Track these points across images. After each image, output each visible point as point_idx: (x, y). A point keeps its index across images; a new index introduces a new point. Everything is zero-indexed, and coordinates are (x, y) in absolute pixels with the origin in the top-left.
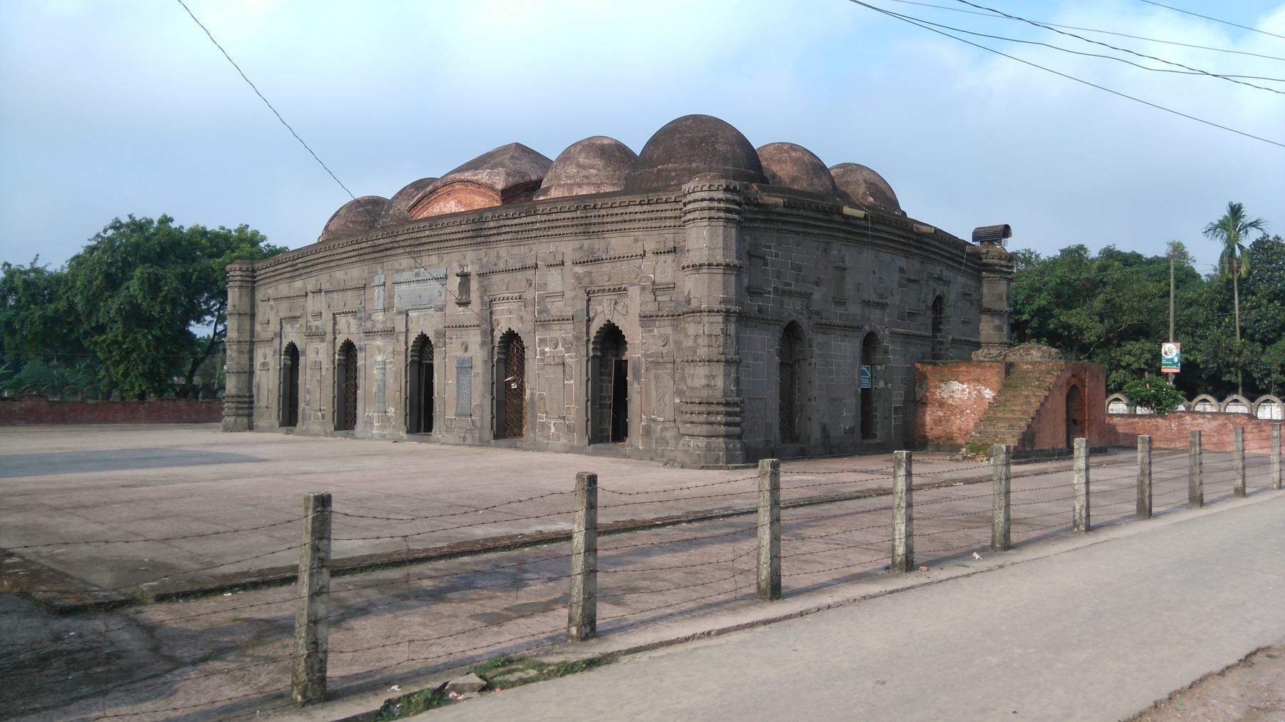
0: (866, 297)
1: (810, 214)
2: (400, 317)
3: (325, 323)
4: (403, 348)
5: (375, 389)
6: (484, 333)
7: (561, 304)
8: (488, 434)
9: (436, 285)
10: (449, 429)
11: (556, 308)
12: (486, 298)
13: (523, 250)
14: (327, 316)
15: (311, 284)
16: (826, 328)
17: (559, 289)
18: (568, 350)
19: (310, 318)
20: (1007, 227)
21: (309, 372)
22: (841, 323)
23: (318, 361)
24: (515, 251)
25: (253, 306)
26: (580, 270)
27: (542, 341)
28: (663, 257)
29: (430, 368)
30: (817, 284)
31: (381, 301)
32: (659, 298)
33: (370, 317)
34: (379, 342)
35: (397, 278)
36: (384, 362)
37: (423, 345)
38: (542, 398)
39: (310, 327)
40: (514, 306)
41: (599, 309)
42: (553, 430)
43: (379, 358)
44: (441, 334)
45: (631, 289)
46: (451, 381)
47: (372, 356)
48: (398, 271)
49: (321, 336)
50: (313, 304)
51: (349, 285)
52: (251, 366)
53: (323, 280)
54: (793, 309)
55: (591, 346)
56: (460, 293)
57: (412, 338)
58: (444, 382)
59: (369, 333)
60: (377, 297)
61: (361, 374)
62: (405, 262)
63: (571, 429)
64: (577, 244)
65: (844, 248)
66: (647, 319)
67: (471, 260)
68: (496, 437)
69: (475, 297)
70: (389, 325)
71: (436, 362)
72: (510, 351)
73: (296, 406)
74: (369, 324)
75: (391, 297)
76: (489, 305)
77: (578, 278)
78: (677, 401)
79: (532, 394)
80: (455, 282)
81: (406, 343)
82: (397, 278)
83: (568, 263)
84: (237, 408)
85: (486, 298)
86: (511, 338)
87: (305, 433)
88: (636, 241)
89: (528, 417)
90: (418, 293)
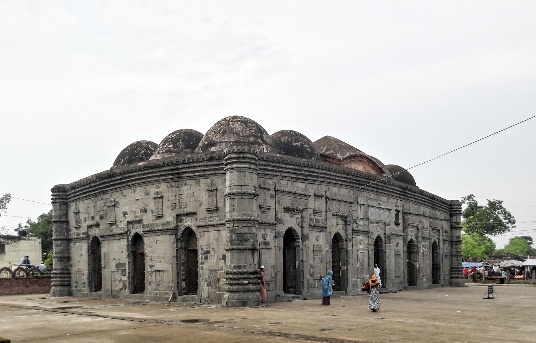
9: (387, 213)
13: (416, 207)
15: (311, 189)
19: (312, 214)
26: (431, 220)
28: (446, 222)
33: (355, 222)
34: (360, 238)
36: (364, 249)
37: (378, 240)
38: (422, 268)
48: (370, 199)
49: (323, 229)
59: (356, 232)
60: (360, 212)
69: (401, 221)
70: (366, 229)
74: (355, 226)
80: (394, 213)
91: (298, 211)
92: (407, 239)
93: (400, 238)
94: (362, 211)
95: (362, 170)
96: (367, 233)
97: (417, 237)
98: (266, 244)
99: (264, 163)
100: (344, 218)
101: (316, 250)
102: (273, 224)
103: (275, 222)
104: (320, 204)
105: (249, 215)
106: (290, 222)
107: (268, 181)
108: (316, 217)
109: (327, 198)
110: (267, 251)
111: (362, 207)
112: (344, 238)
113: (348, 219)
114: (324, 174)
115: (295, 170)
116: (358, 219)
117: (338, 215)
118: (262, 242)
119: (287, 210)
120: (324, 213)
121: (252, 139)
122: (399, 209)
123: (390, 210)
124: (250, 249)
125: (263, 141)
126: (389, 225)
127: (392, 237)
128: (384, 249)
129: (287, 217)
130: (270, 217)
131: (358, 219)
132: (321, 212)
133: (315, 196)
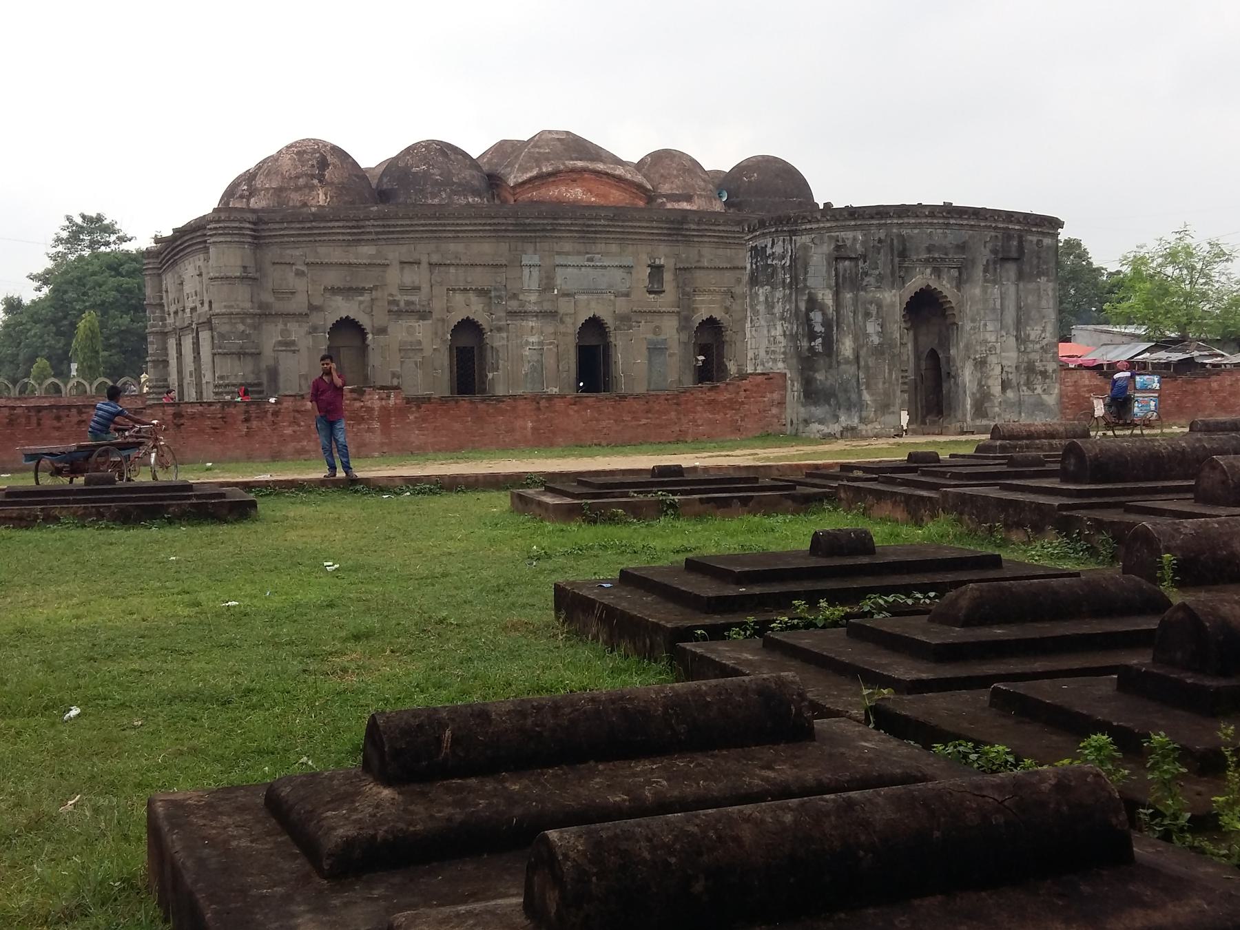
5: (526, 368)
9: (620, 273)
12: (688, 289)
15: (394, 253)
24: (720, 252)
25: (259, 269)
34: (532, 323)
35: (559, 260)
36: (541, 343)
37: (594, 325)
39: (396, 303)
43: (532, 339)
44: (625, 320)
46: (641, 361)
48: (558, 253)
49: (424, 315)
62: (568, 246)
70: (547, 306)
76: (686, 296)
82: (559, 260)
91: (361, 291)
92: (687, 319)
96: (552, 315)
97: (727, 310)
98: (288, 345)
99: (277, 226)
100: (482, 292)
101: (407, 350)
102: (300, 314)
103: (306, 311)
105: (232, 307)
106: (343, 308)
107: (288, 252)
108: (406, 298)
109: (430, 264)
110: (290, 354)
112: (485, 326)
113: (493, 294)
114: (423, 225)
115: (350, 228)
116: (522, 291)
117: (465, 289)
118: (280, 343)
119: (334, 291)
120: (425, 287)
121: (301, 181)
123: (628, 269)
124: (252, 354)
125: (320, 181)
126: (627, 295)
128: (612, 339)
129: (339, 300)
130: (298, 304)
131: (522, 291)
132: (419, 288)
133: (402, 263)
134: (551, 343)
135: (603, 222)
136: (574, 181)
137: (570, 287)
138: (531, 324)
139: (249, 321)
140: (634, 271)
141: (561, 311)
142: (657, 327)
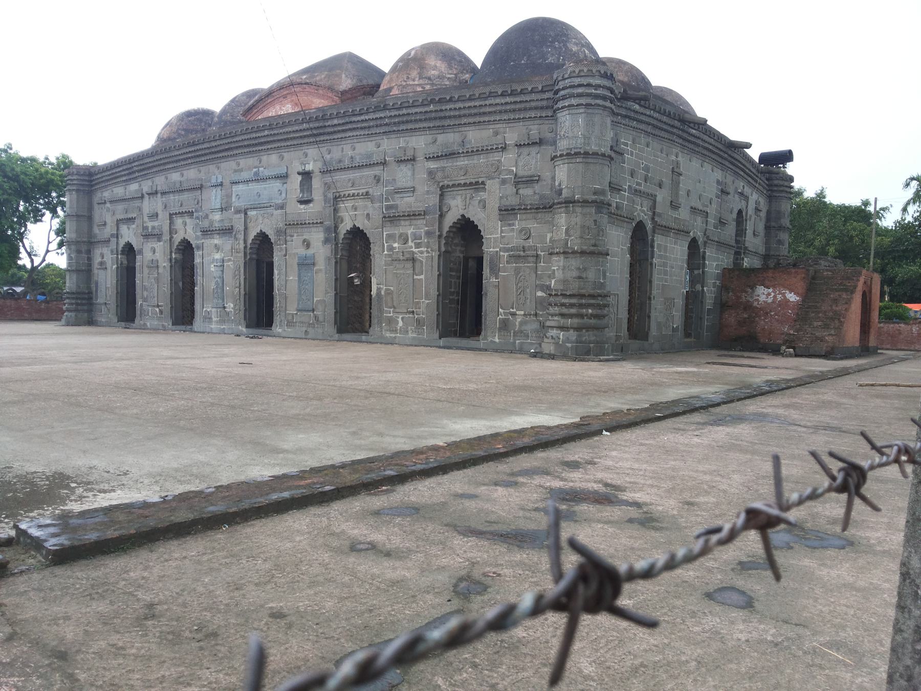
0: (693, 204)
1: (656, 115)
2: (238, 216)
3: (162, 223)
4: (242, 246)
5: (213, 286)
6: (327, 230)
7: (411, 200)
8: (331, 329)
10: (290, 324)
11: (406, 203)
14: (163, 217)
15: (146, 186)
16: (666, 230)
17: (410, 184)
18: (418, 245)
19: (146, 219)
20: (790, 152)
21: (146, 270)
22: (676, 227)
23: (155, 257)
26: (432, 165)
27: (391, 237)
28: (525, 150)
29: (270, 266)
30: (660, 186)
31: (218, 200)
32: (521, 191)
33: (207, 216)
34: (217, 241)
38: (389, 293)
39: (147, 228)
40: (360, 203)
41: (453, 203)
42: (401, 324)
43: (218, 256)
44: (279, 232)
45: (488, 183)
46: (293, 278)
47: (209, 255)
49: (159, 237)
50: (147, 206)
51: (185, 186)
52: (90, 265)
53: (160, 182)
54: (641, 211)
55: (443, 242)
56: (302, 191)
57: (252, 235)
58: (285, 280)
59: (207, 233)
60: (214, 198)
61: (198, 271)
63: (419, 323)
64: (429, 138)
65: (680, 154)
66: (507, 212)
67: (311, 159)
68: (340, 331)
70: (227, 224)
71: (276, 259)
72: (355, 249)
73: (134, 302)
75: (229, 196)
77: (431, 173)
78: (539, 294)
79: (379, 289)
81: (245, 241)
83: (420, 158)
84: (77, 304)
85: (330, 196)
86: (358, 236)
87: (143, 328)
88: (496, 133)
89: (374, 312)
90: (260, 192)
93: (314, 230)
94: (219, 197)
95: (290, 111)
104: (157, 204)
111: (219, 188)
116: (213, 211)
122: (309, 167)
123: (284, 177)
126: (282, 207)
127: (288, 231)
131: (213, 211)
133: (148, 194)
134: (229, 260)
135: (266, 133)
136: (285, 97)
137: (241, 204)
138: (216, 241)
139: (73, 247)
140: (289, 180)
141: (235, 229)
142: (304, 241)
